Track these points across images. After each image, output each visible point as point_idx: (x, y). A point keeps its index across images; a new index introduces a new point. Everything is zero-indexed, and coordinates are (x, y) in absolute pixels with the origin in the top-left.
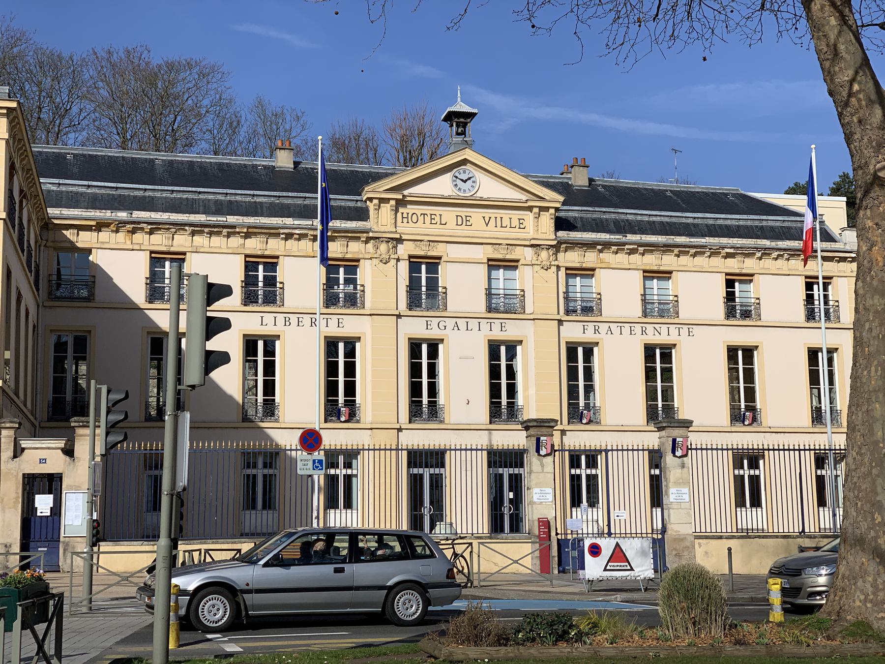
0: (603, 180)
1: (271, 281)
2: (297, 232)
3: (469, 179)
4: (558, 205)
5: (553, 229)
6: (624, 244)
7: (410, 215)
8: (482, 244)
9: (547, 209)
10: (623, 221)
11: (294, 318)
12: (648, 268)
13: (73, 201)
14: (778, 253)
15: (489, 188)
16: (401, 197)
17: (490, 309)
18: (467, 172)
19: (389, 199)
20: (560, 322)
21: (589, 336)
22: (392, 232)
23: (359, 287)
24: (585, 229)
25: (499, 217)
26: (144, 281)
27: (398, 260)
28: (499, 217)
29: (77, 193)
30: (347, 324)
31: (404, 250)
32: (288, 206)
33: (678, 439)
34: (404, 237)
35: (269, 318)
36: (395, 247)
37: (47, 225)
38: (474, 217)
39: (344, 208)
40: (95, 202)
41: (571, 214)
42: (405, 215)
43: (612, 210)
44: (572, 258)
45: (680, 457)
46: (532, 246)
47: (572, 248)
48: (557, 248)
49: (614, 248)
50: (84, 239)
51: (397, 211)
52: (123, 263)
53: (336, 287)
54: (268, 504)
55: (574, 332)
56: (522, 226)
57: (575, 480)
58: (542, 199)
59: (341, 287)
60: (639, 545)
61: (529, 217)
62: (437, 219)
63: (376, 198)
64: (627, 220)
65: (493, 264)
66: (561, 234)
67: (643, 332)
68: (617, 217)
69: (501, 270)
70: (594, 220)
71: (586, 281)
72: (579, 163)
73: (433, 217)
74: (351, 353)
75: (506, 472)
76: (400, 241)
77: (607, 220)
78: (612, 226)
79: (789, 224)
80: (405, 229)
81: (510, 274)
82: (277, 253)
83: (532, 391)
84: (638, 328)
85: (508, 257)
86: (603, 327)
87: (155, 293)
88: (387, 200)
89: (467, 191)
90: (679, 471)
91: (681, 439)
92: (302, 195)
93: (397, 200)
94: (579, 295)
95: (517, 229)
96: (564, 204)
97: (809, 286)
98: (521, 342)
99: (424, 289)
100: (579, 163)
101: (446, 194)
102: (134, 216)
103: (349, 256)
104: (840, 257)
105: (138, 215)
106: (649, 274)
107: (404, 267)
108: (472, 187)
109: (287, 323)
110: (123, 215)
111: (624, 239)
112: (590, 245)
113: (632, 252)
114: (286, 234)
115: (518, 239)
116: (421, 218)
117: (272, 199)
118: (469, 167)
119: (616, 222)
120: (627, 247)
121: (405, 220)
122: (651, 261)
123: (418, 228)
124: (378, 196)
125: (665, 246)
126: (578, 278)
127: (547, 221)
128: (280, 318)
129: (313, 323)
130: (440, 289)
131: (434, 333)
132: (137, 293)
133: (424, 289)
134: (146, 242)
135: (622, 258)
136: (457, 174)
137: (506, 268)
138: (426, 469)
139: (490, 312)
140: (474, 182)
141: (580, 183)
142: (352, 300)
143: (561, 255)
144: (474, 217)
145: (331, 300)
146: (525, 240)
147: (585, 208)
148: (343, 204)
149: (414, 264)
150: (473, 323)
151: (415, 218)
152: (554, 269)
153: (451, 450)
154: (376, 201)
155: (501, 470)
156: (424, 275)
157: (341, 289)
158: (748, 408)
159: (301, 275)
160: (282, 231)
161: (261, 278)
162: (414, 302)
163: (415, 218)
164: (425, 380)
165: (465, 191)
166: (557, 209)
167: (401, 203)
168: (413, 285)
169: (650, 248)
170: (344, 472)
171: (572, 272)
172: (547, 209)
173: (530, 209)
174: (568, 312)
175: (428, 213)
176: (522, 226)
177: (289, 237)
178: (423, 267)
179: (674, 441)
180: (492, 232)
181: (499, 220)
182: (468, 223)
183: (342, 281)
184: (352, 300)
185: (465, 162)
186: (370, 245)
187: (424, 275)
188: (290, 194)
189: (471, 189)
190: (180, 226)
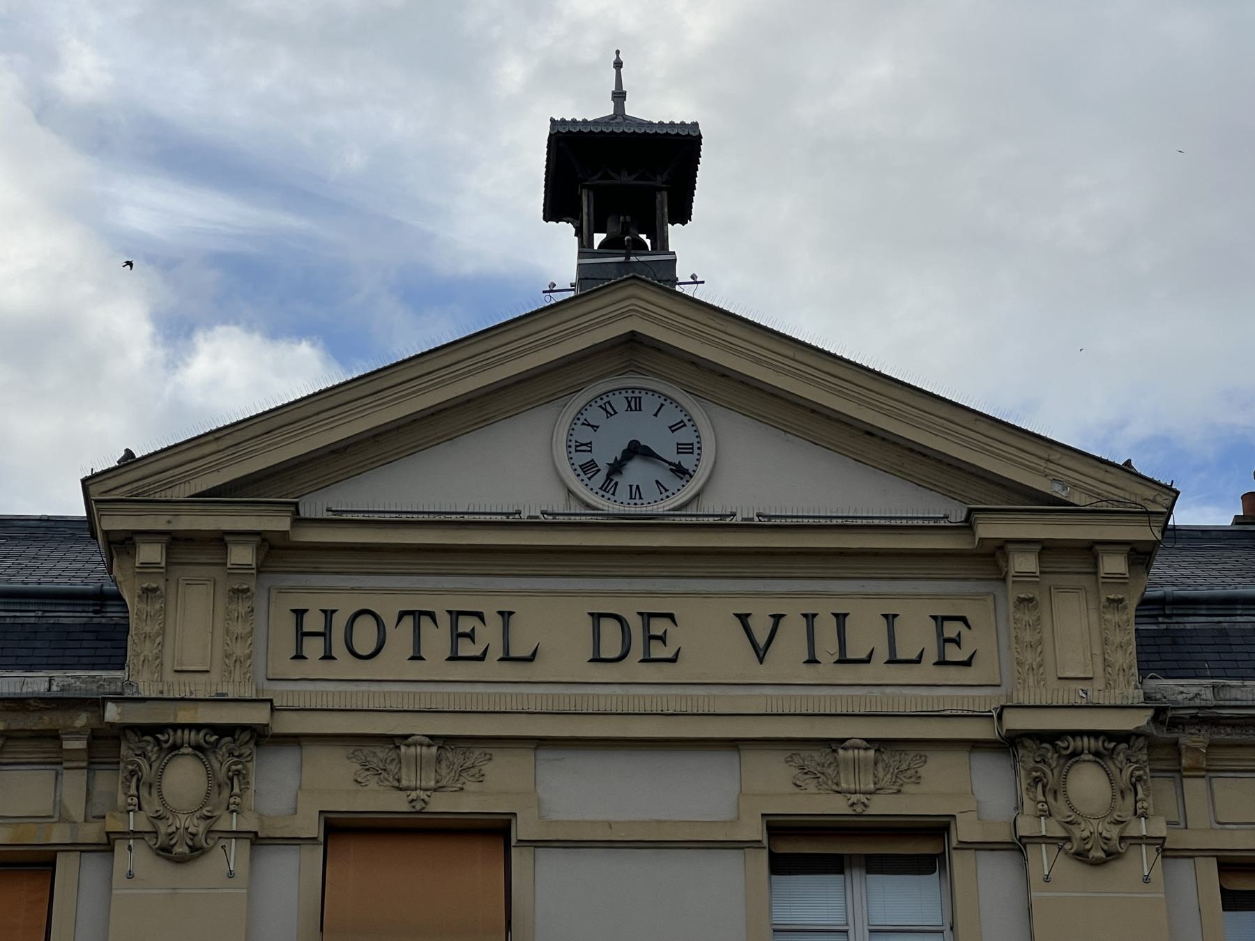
7: (339, 623)
8: (733, 744)
16: (281, 523)
19: (220, 540)
25: (825, 612)
28: (825, 612)
42: (314, 622)
46: (1010, 744)
56: (953, 653)
62: (489, 634)
63: (151, 535)
66: (1183, 691)
73: (465, 625)
85: (883, 806)
95: (927, 671)
116: (399, 638)
121: (314, 647)
124: (160, 524)
151: (365, 637)
154: (150, 553)
163: (365, 637)
175: (441, 606)
176: (953, 653)
180: (791, 688)
182: (658, 651)
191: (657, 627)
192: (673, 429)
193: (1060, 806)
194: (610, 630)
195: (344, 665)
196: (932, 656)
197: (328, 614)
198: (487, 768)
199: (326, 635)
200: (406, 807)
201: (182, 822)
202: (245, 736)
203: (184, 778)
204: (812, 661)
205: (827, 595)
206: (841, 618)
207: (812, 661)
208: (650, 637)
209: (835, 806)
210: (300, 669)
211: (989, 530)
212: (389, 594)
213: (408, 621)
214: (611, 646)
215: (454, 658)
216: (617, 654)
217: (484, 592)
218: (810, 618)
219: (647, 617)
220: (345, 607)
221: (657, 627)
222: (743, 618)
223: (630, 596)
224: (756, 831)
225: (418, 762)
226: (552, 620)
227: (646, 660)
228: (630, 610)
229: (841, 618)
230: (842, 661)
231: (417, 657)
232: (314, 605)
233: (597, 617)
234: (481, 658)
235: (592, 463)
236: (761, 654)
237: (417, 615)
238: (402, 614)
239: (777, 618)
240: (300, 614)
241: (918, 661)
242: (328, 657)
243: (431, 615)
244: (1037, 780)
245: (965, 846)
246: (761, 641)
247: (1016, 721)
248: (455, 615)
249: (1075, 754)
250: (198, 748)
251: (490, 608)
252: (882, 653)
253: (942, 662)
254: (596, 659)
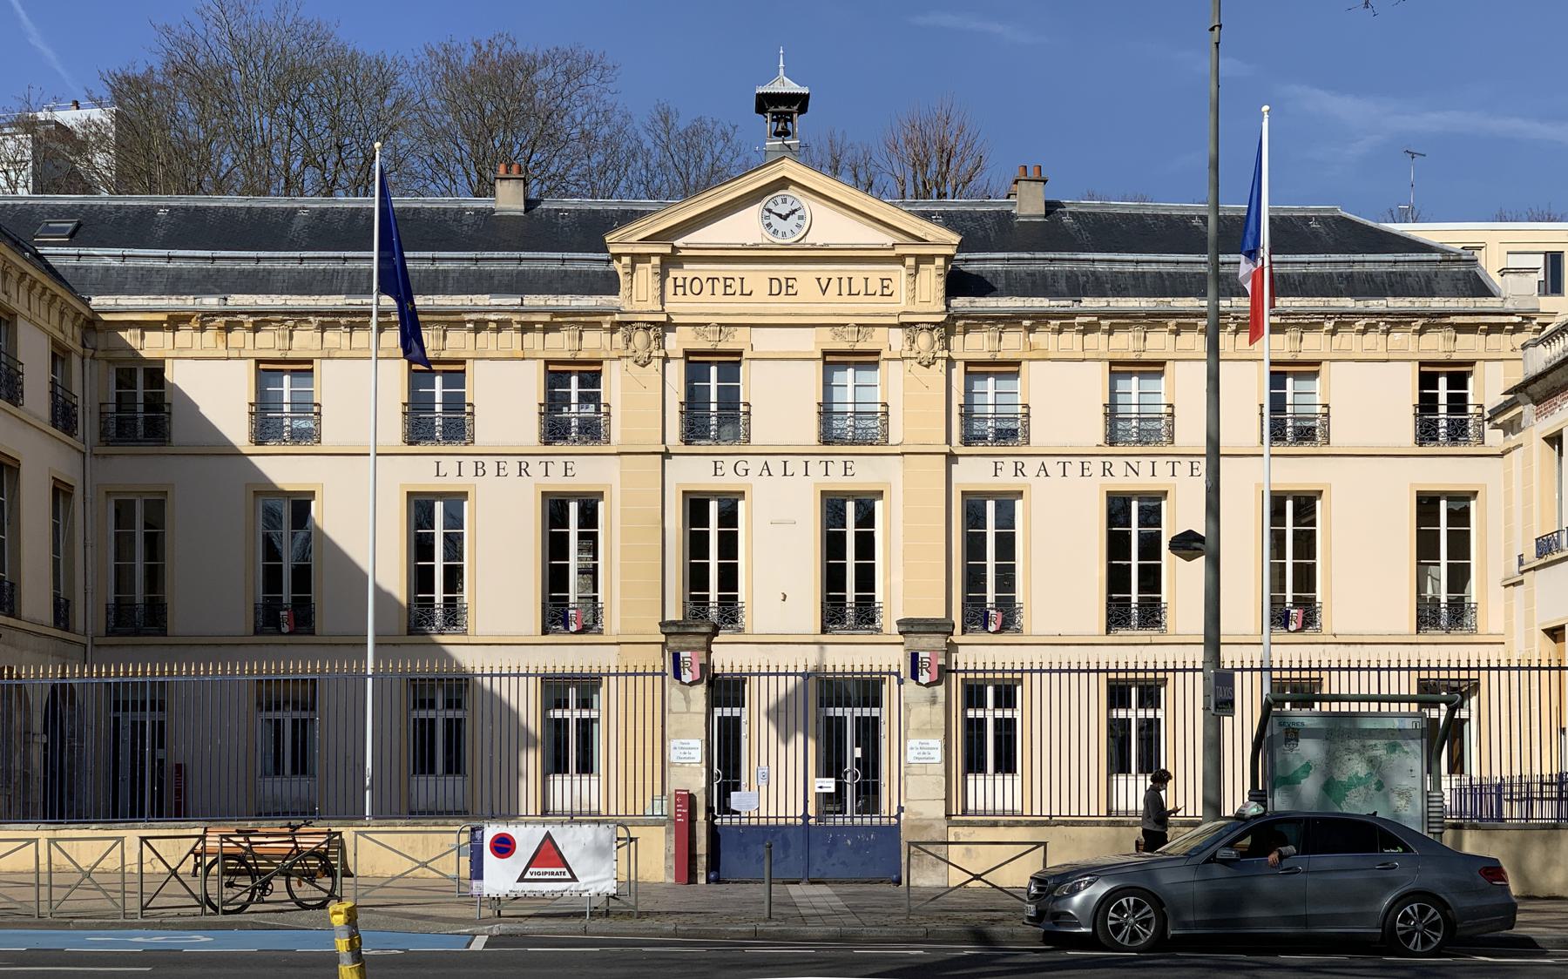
0: (1077, 202)
1: (456, 404)
2: (492, 317)
3: (793, 212)
4: (950, 251)
5: (941, 294)
6: (1073, 315)
9: (930, 259)
10: (1085, 274)
11: (490, 463)
12: (1118, 356)
13: (144, 282)
14: (1421, 321)
15: (830, 227)
16: (668, 250)
17: (827, 438)
18: (789, 200)
20: (951, 458)
21: (1006, 480)
22: (654, 312)
23: (603, 409)
24: (1010, 292)
25: (845, 276)
26: (246, 409)
27: (666, 359)
28: (845, 276)
29: (150, 270)
30: (582, 471)
31: (676, 342)
32: (491, 275)
33: (921, 654)
34: (676, 319)
35: (449, 464)
36: (661, 338)
37: (92, 325)
38: (803, 278)
39: (587, 274)
40: (177, 284)
41: (989, 266)
43: (1066, 255)
44: (977, 344)
45: (928, 685)
46: (902, 325)
47: (977, 327)
48: (948, 327)
49: (1055, 323)
50: (152, 345)
51: (663, 276)
52: (213, 382)
53: (565, 409)
54: (454, 766)
55: (975, 473)
56: (886, 292)
57: (974, 729)
58: (922, 241)
59: (574, 408)
60: (590, 837)
61: (899, 274)
62: (736, 285)
63: (626, 255)
64: (1093, 273)
65: (833, 361)
66: (959, 303)
67: (1107, 471)
68: (1075, 267)
69: (850, 371)
70: (1032, 274)
71: (1005, 385)
72: (1032, 174)
74: (866, 518)
75: (850, 714)
76: (669, 326)
77: (1054, 273)
78: (1062, 285)
79: (1407, 267)
80: (678, 305)
81: (865, 376)
82: (462, 355)
83: (898, 578)
84: (1096, 465)
86: (1032, 465)
87: (265, 426)
88: (645, 258)
89: (789, 234)
90: (926, 709)
91: (927, 654)
92: (516, 254)
93: (662, 255)
94: (991, 409)
95: (877, 298)
96: (961, 247)
97: (1427, 380)
98: (880, 494)
99: (713, 407)
100: (1032, 174)
101: (750, 242)
102: (229, 302)
103: (582, 355)
104: (1489, 325)
105: (238, 300)
106: (1120, 369)
107: (676, 371)
108: (799, 226)
109: (479, 470)
110: (211, 302)
111: (1076, 307)
112: (1011, 320)
113: (1087, 329)
114: (476, 322)
115: (878, 315)
116: (708, 286)
117: (466, 264)
118: (792, 191)
119: (1071, 277)
120: (1078, 320)
121: (680, 290)
122: (1125, 344)
123: (699, 302)
124: (628, 250)
125: (1149, 315)
126: (991, 380)
127: (931, 282)
128: (468, 463)
129: (523, 471)
130: (742, 408)
131: (728, 481)
132: (235, 426)
133: (713, 407)
134: (249, 345)
135: (1070, 341)
136: (771, 205)
137: (858, 366)
138: (848, 710)
139: (825, 443)
140: (801, 218)
141: (1029, 211)
142: (592, 431)
143: (956, 341)
144: (803, 278)
145: (554, 431)
146: (891, 315)
147: (1016, 255)
148: (585, 267)
149: (696, 364)
150: (796, 464)
152: (941, 364)
153: (609, 675)
155: (839, 712)
156: (714, 384)
157: (574, 411)
158: (1297, 602)
159: (504, 389)
160: (467, 317)
161: (438, 398)
162: (694, 429)
163: (696, 288)
164: (713, 561)
165: (784, 234)
166: (949, 258)
167: (671, 261)
168: (694, 402)
169: (1123, 320)
170: (577, 714)
171: (977, 370)
172: (930, 259)
173: (900, 259)
174: (967, 441)
175: (721, 275)
176: (886, 292)
177: (480, 326)
178: (713, 370)
179: (915, 656)
180: (834, 304)
181: (845, 282)
182: (791, 291)
183: (574, 398)
184: (592, 431)
185: (784, 183)
186: (618, 337)
187: (714, 384)
188: (496, 255)
189: (796, 230)
190: (300, 316)
191: (790, 282)
203: (640, 338)
208: (787, 287)
209: (845, 346)
211: (900, 251)
214: (775, 290)
223: (782, 271)
226: (757, 277)
247: (904, 319)
251: (737, 276)
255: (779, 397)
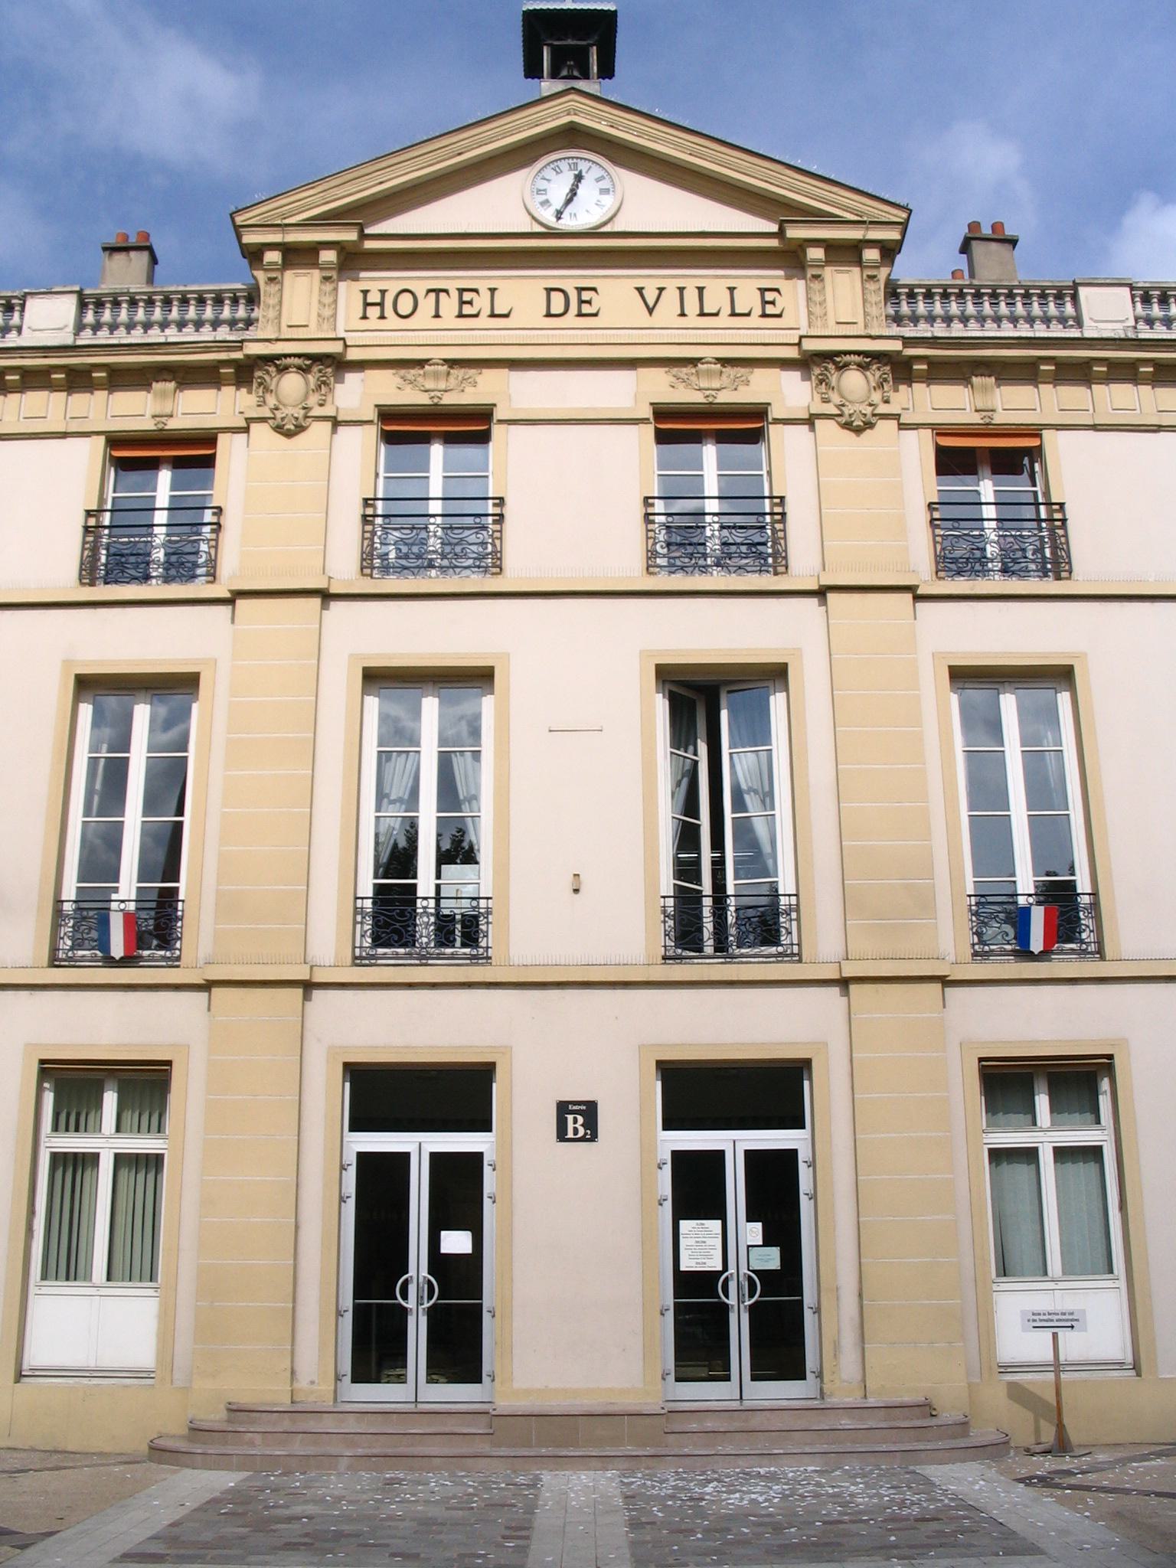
16: (351, 236)
31: (357, 395)
42: (374, 297)
56: (770, 309)
62: (482, 302)
63: (272, 246)
65: (676, 426)
73: (467, 296)
116: (427, 305)
151: (405, 304)
163: (405, 304)
175: (452, 286)
176: (770, 309)
180: (669, 329)
181: (691, 297)
182: (586, 309)
191: (586, 296)
192: (598, 180)
193: (835, 398)
194: (557, 297)
195: (393, 321)
196: (758, 311)
197: (383, 292)
198: (479, 379)
199: (381, 304)
200: (429, 402)
201: (289, 411)
202: (329, 361)
203: (292, 385)
204: (683, 314)
205: (691, 277)
206: (701, 290)
207: (683, 314)
208: (583, 304)
209: (695, 397)
210: (365, 324)
212: (420, 280)
213: (433, 295)
214: (557, 306)
215: (461, 316)
216: (561, 311)
217: (480, 279)
218: (681, 289)
219: (580, 290)
220: (393, 288)
221: (586, 296)
222: (640, 290)
223: (569, 279)
224: (648, 413)
225: (436, 376)
226: (522, 292)
227: (580, 315)
228: (570, 287)
229: (701, 290)
230: (702, 314)
231: (437, 316)
232: (374, 287)
233: (549, 290)
234: (476, 316)
235: (547, 201)
236: (651, 311)
237: (437, 291)
238: (430, 291)
239: (661, 290)
240: (365, 292)
241: (748, 315)
242: (382, 317)
243: (446, 291)
244: (821, 382)
245: (777, 421)
246: (651, 305)
247: (809, 345)
248: (461, 291)
249: (846, 365)
250: (299, 368)
251: (483, 286)
252: (726, 310)
253: (764, 315)
254: (549, 315)
255: (574, 483)
